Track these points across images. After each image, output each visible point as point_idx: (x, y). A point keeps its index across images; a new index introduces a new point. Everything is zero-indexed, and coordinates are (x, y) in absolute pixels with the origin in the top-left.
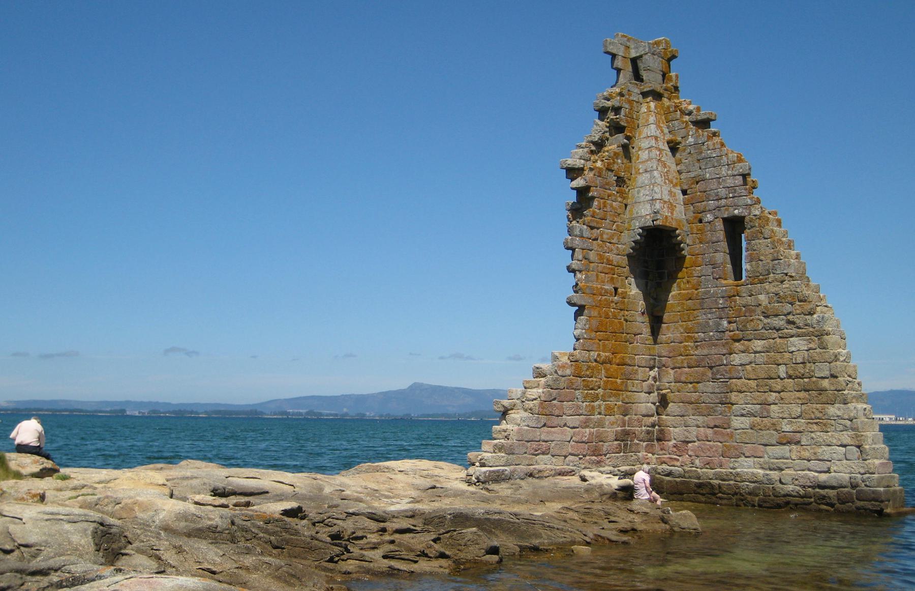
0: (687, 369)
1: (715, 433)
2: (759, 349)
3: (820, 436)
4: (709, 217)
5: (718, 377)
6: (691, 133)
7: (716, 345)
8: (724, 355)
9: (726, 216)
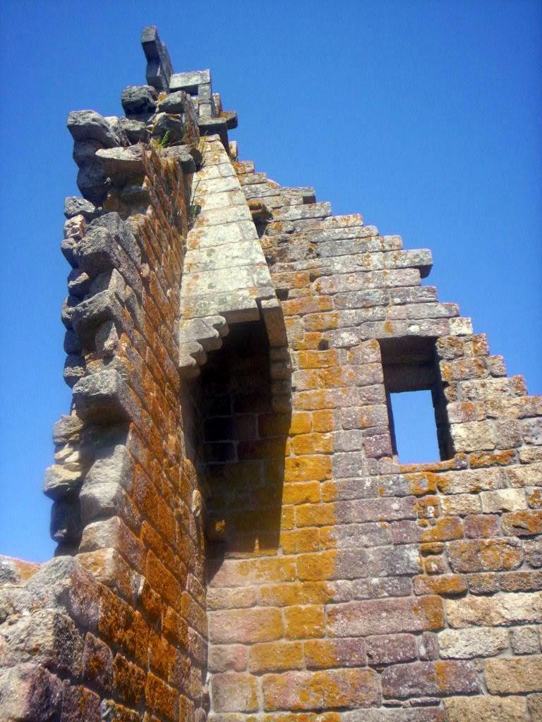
0: (305, 675)
2: (520, 614)
4: (347, 337)
5: (405, 691)
7: (390, 610)
8: (418, 632)
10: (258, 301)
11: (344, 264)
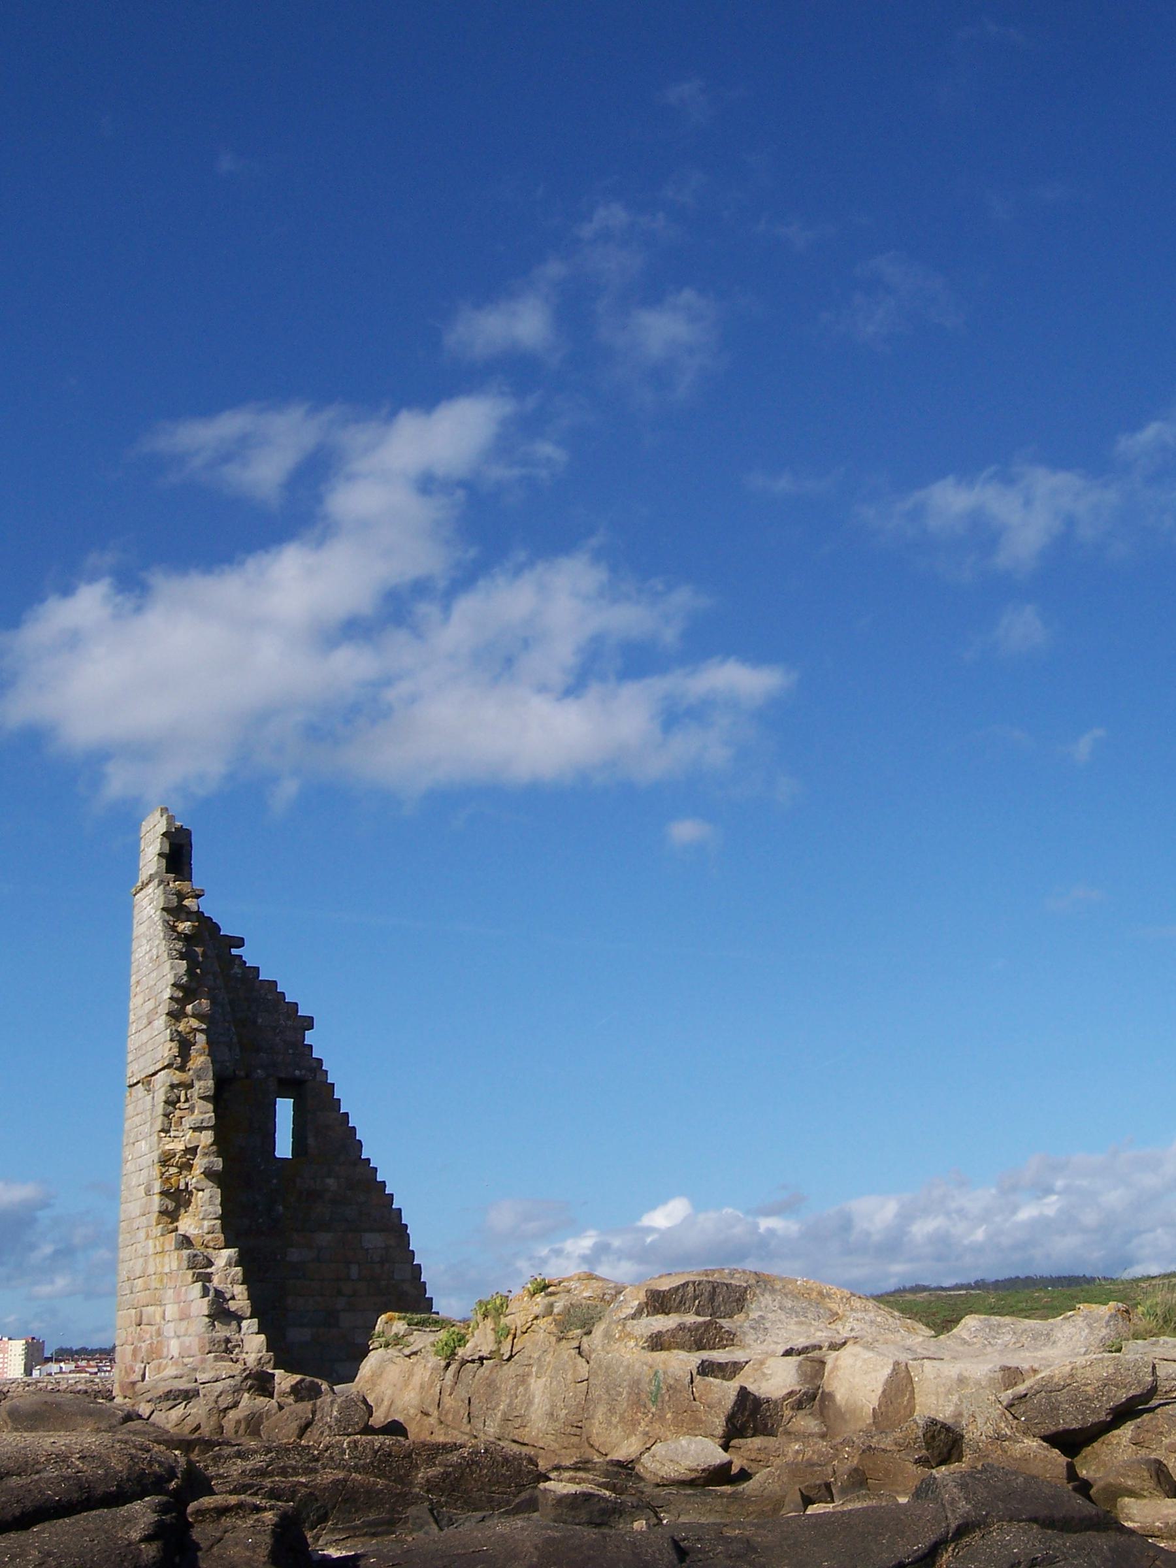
9: (283, 1075)
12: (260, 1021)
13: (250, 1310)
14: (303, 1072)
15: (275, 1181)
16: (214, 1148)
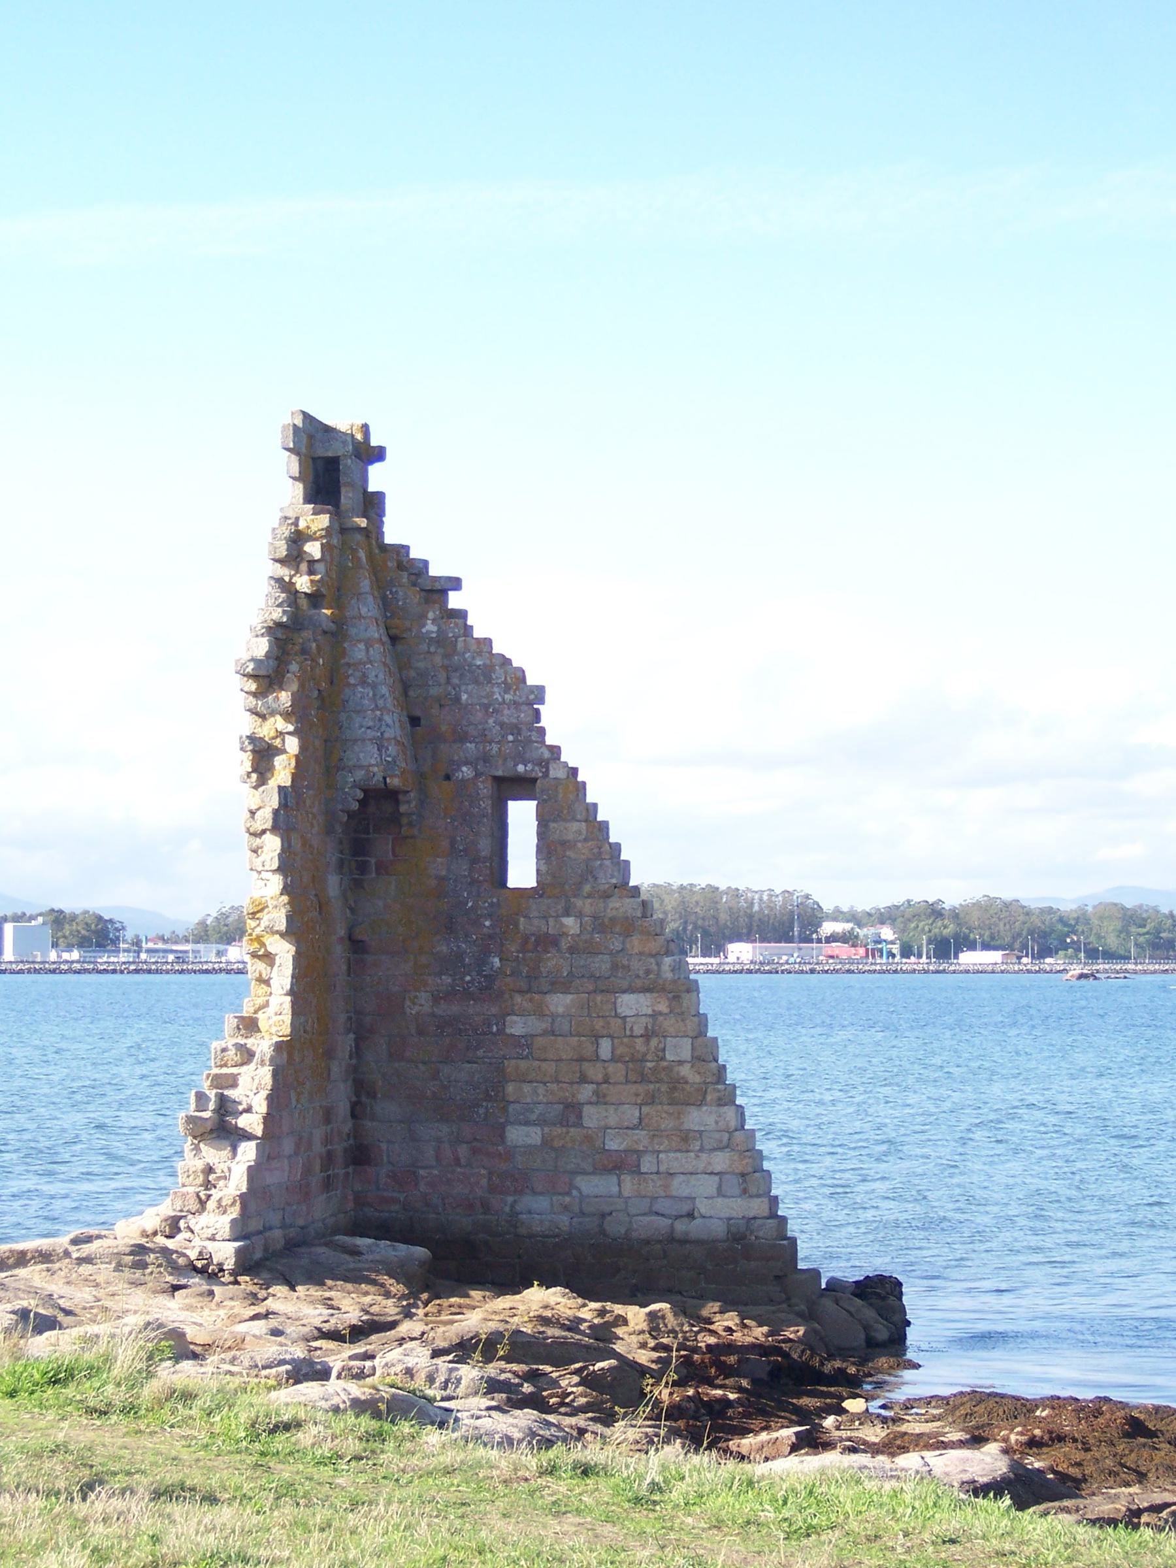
1: (475, 1151)
2: (561, 1010)
3: (672, 1161)
4: (466, 771)
6: (431, 615)
9: (500, 773)
10: (385, 778)
11: (470, 695)
12: (464, 697)
13: (262, 1126)
14: (530, 767)
15: (487, 923)
16: (285, 898)
